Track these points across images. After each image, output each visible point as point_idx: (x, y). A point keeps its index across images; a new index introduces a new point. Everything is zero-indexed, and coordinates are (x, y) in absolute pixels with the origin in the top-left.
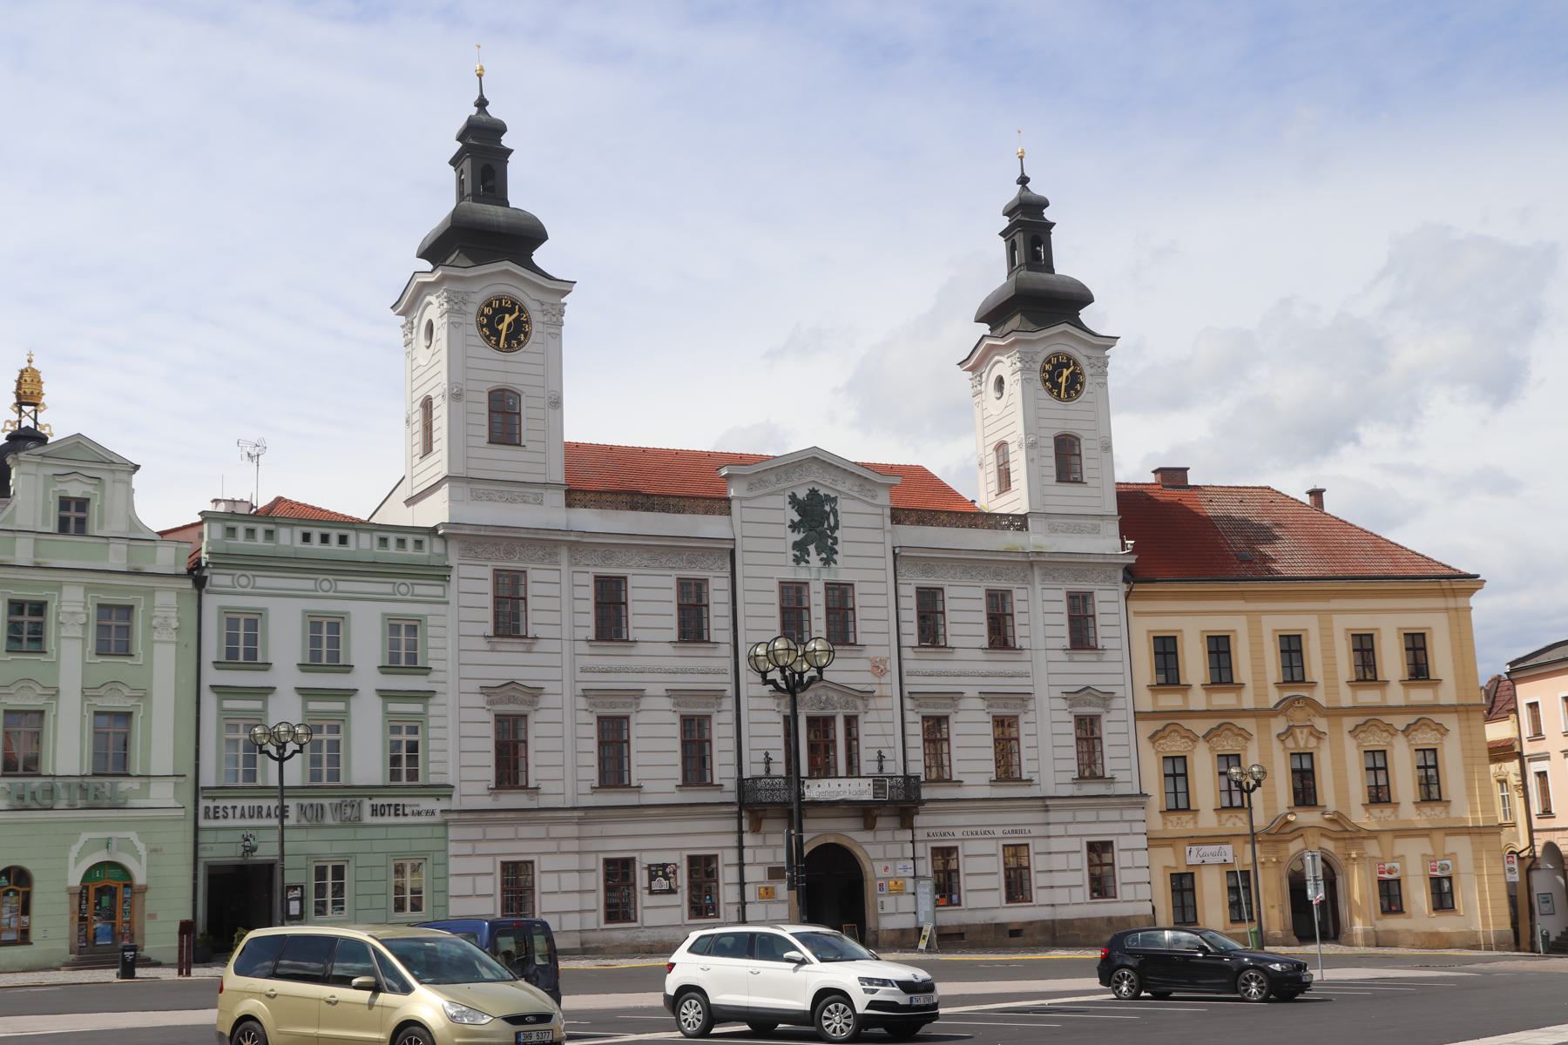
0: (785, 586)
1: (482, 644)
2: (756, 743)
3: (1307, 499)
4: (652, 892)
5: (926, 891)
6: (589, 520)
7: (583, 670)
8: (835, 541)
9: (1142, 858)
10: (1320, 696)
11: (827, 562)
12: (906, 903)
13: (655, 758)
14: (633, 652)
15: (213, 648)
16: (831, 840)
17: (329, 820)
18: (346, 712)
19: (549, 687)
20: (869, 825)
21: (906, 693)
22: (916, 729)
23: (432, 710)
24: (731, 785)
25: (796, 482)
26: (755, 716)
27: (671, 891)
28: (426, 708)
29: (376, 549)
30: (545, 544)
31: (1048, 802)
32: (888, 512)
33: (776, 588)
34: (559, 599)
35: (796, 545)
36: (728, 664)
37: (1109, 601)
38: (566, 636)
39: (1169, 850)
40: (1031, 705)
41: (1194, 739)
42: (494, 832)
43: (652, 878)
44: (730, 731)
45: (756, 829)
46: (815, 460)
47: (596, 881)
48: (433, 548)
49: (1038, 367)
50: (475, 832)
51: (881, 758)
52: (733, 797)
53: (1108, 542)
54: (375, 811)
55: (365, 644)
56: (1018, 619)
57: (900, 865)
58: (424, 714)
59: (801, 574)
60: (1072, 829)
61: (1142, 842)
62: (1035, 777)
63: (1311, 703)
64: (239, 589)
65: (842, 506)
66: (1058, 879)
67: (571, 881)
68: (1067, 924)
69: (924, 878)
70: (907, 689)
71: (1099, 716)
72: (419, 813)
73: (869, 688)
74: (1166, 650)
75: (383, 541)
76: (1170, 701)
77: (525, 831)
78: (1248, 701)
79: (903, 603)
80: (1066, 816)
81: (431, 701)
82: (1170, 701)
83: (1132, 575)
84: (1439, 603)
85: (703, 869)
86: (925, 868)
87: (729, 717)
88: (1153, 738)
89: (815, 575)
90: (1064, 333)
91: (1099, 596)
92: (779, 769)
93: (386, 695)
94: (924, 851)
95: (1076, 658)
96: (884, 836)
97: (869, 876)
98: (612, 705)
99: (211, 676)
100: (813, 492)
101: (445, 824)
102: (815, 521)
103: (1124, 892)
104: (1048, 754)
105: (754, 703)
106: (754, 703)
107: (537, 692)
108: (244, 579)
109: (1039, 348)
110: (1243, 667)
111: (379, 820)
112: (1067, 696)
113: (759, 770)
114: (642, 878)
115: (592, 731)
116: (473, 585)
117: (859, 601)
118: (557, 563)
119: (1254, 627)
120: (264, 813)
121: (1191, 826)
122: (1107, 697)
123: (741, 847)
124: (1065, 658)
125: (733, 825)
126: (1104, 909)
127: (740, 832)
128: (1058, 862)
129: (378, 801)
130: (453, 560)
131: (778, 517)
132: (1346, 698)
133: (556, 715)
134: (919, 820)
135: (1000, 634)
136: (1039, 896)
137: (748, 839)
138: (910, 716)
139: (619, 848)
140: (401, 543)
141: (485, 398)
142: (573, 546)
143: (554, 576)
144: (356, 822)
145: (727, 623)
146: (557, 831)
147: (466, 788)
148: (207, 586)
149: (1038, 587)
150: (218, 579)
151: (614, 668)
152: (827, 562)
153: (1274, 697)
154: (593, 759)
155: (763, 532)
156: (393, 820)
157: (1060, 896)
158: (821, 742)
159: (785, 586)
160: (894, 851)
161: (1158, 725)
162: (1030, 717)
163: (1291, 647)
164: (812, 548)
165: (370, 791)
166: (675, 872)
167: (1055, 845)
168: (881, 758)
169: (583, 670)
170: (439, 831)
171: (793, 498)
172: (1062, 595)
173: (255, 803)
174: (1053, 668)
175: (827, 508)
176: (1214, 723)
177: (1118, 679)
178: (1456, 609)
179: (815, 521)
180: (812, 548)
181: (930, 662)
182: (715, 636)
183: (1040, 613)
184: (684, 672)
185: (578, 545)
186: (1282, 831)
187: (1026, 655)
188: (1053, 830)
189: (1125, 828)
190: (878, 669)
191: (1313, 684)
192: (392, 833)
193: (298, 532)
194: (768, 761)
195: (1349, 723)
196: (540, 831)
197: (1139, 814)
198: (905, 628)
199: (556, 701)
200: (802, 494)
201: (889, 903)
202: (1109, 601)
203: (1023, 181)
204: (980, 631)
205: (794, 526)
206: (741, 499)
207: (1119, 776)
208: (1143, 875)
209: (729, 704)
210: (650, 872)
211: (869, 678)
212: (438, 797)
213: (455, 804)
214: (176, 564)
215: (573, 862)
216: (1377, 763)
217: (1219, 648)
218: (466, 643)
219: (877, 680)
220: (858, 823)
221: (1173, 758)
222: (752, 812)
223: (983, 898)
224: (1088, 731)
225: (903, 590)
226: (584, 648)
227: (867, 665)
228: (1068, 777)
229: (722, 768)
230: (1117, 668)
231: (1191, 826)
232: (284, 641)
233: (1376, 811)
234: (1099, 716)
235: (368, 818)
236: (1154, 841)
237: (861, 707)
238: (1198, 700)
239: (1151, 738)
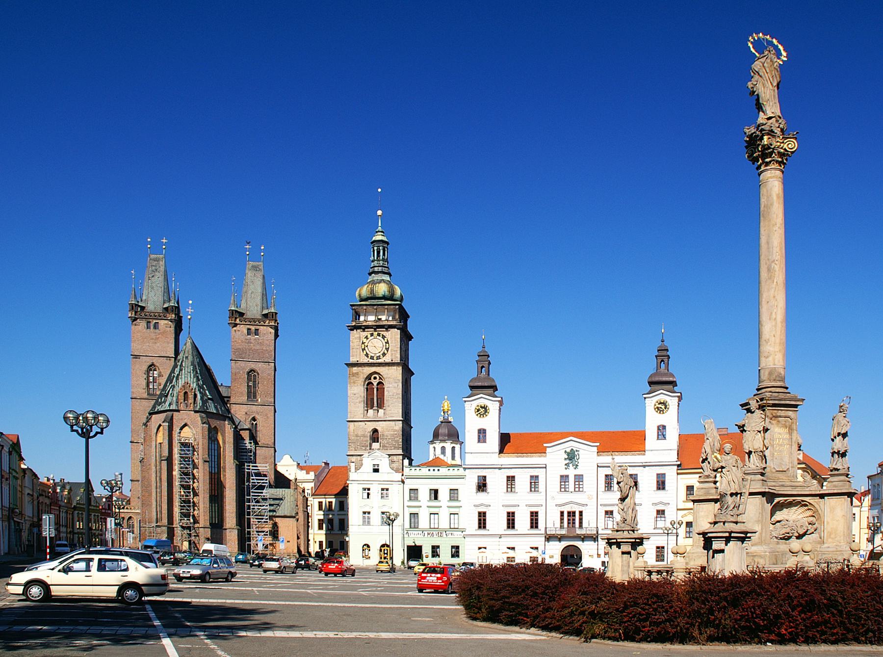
13: (523, 521)
53: (673, 457)
55: (444, 495)
59: (565, 473)
89: (571, 472)
92: (558, 525)
150: (406, 481)
151: (511, 498)
158: (572, 517)
200: (568, 450)
202: (671, 473)
232: (424, 495)
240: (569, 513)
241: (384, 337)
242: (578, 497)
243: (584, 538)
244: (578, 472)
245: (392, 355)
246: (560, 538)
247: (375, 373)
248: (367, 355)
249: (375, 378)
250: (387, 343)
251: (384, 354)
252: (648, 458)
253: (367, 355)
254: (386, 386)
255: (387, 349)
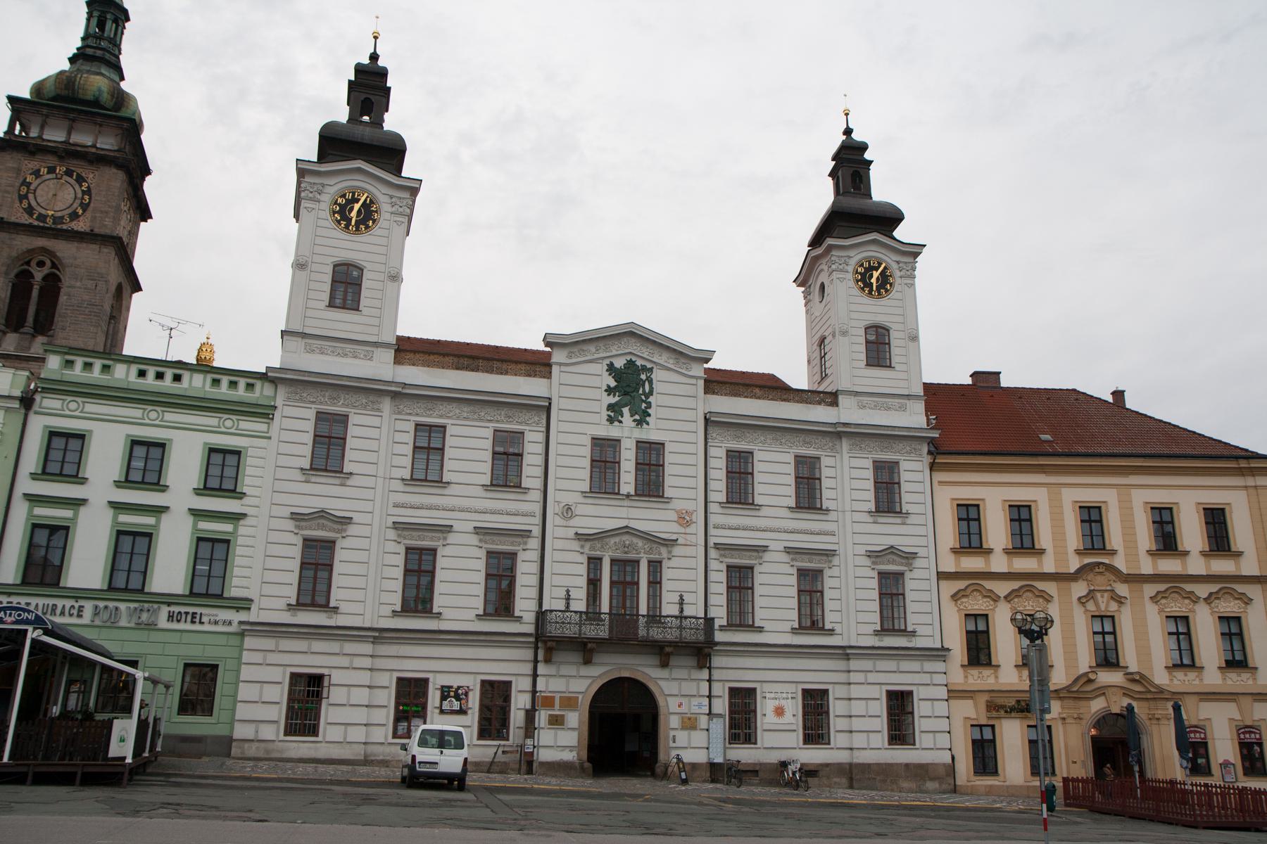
0: (597, 442)
1: (298, 475)
2: (558, 580)
3: (1110, 399)
4: (442, 712)
5: (719, 728)
6: (416, 375)
7: (396, 506)
8: (649, 405)
9: (942, 708)
10: (1120, 563)
11: (639, 423)
12: (698, 738)
13: (460, 590)
14: (446, 492)
15: (32, 458)
16: (626, 674)
17: (123, 623)
18: (156, 526)
19: (357, 517)
20: (664, 665)
21: (711, 544)
22: (719, 578)
23: (242, 530)
24: (530, 617)
25: (615, 352)
26: (559, 556)
27: (462, 712)
28: (236, 529)
29: (208, 388)
30: (369, 391)
31: (849, 651)
32: (701, 383)
33: (588, 442)
34: (379, 441)
35: (611, 407)
36: (537, 509)
37: (913, 471)
38: (381, 473)
39: (970, 702)
40: (836, 561)
41: (996, 599)
42: (287, 644)
43: (443, 698)
44: (535, 568)
45: (548, 661)
46: (631, 333)
47: (388, 697)
48: (262, 392)
49: (850, 269)
50: (268, 643)
51: (681, 602)
52: (530, 629)
53: (915, 417)
54: (171, 617)
56: (826, 483)
57: (695, 701)
58: (234, 533)
59: (613, 431)
60: (872, 677)
61: (943, 693)
62: (838, 628)
63: (1111, 569)
64: (67, 412)
65: (658, 375)
66: (857, 724)
67: (361, 696)
68: (865, 768)
69: (719, 716)
70: (712, 541)
71: (902, 574)
72: (216, 623)
73: (674, 537)
74: (969, 515)
75: (216, 382)
76: (972, 563)
77: (319, 646)
78: (1049, 566)
79: (713, 463)
80: (866, 664)
81: (242, 522)
82: (972, 563)
83: (936, 449)
84: (1238, 481)
85: (496, 696)
86: (722, 706)
87: (535, 555)
88: (955, 597)
90: (874, 242)
91: (904, 465)
92: (580, 605)
93: (197, 514)
94: (721, 690)
95: (881, 520)
96: (678, 673)
97: (662, 710)
98: (420, 538)
99: (26, 485)
100: (630, 363)
101: (242, 634)
102: (630, 388)
103: (923, 740)
104: (852, 607)
105: (560, 544)
106: (560, 544)
107: (348, 521)
108: (73, 404)
109: (852, 253)
110: (1044, 535)
111: (175, 626)
112: (871, 555)
113: (561, 605)
114: (434, 698)
115: (400, 560)
116: (295, 424)
117: (669, 458)
118: (378, 410)
119: (1056, 500)
120: (58, 611)
121: (991, 680)
122: (910, 557)
123: (535, 676)
124: (871, 520)
125: (529, 654)
126: (902, 755)
127: (536, 661)
128: (858, 707)
129: (176, 609)
130: (279, 402)
131: (596, 381)
132: (1147, 567)
133: (363, 543)
134: (717, 661)
135: (808, 492)
136: (838, 739)
137: (541, 669)
138: (713, 565)
139: (413, 669)
140: (233, 384)
141: (329, 270)
142: (395, 396)
143: (375, 421)
144: (151, 626)
145: (539, 472)
146: (350, 647)
147: (265, 603)
148: (36, 407)
149: (846, 456)
152: (639, 423)
153: (1074, 564)
154: (398, 586)
155: (581, 397)
156: (189, 627)
157: (859, 741)
159: (597, 442)
160: (689, 688)
161: (961, 584)
162: (835, 572)
163: (1092, 517)
164: (626, 410)
165: (168, 599)
166: (466, 694)
167: (856, 691)
168: (681, 602)
169: (396, 506)
170: (235, 641)
171: (611, 368)
172: (869, 464)
173: (51, 601)
174: (858, 528)
175: (643, 377)
176: (1016, 585)
177: (923, 541)
178: (1256, 487)
179: (630, 388)
180: (626, 410)
181: (739, 518)
182: (526, 483)
183: (849, 478)
184: (493, 512)
185: (400, 395)
186: (1080, 689)
187: (832, 516)
188: (854, 677)
189: (925, 678)
190: (684, 519)
191: (1113, 553)
192: (186, 636)
193: (134, 369)
194: (568, 599)
195: (1150, 589)
196: (334, 646)
197: (939, 666)
198: (713, 485)
199: (364, 531)
200: (619, 363)
201: (682, 737)
203: (848, 132)
204: (788, 494)
205: (610, 391)
206: (560, 364)
207: (921, 630)
208: (944, 725)
209: (534, 543)
210: (442, 692)
211: (675, 527)
212: (238, 609)
213: (253, 616)
214: (12, 387)
215: (364, 677)
216: (1181, 629)
217: (1021, 516)
218: (281, 474)
219: (682, 530)
220: (655, 660)
221: (976, 616)
222: (545, 642)
223: (779, 735)
224: (891, 590)
225: (713, 452)
226: (398, 485)
227: (674, 516)
228: (870, 629)
229: (525, 604)
230: (922, 531)
231: (991, 680)
233: (1179, 675)
234: (902, 574)
235: (163, 622)
236: (955, 694)
237: (665, 555)
238: (999, 563)
239: (952, 596)
240: (613, 561)
241: (80, 180)
242: (648, 518)
243: (664, 652)
244: (651, 433)
245: (94, 218)
246: (586, 649)
247: (44, 250)
248: (30, 210)
249: (41, 264)
250: (88, 192)
251: (74, 216)
252: (848, 413)
253: (30, 210)
254: (67, 281)
255: (85, 207)
